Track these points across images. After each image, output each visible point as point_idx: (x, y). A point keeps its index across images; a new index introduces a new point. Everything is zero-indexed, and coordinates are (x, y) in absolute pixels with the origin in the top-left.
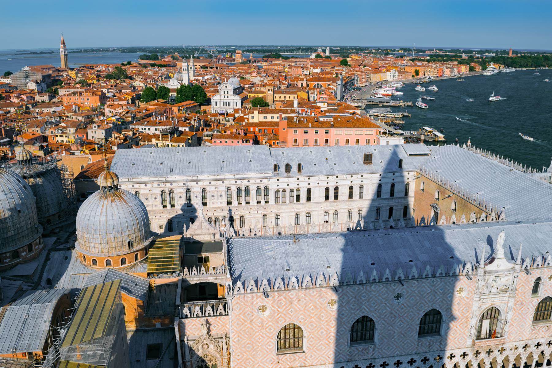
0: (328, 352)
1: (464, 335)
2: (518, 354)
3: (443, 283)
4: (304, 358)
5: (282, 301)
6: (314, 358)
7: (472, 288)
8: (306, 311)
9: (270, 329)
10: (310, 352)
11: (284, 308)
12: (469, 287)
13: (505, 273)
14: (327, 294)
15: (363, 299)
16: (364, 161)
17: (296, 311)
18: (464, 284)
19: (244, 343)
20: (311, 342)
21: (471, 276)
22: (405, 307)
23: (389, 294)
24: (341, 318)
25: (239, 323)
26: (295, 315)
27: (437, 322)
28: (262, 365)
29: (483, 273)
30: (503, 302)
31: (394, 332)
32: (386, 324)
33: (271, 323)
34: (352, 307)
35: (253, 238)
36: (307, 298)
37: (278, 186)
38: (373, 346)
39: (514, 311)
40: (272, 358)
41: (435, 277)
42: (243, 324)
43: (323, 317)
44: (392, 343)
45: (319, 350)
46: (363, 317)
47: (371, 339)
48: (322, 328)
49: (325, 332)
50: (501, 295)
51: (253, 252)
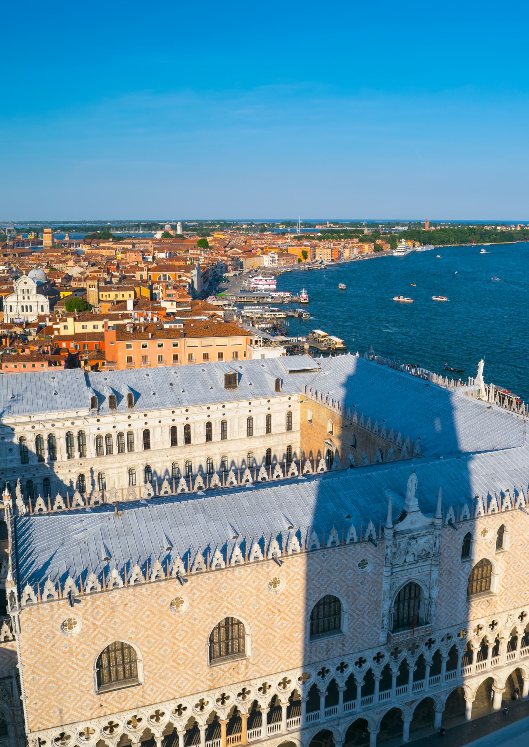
0: (175, 681)
1: (375, 628)
2: (452, 645)
3: (337, 555)
4: (141, 693)
6: (157, 691)
7: (379, 559)
8: (138, 620)
9: (84, 655)
10: (149, 682)
11: (102, 620)
12: (375, 557)
13: (423, 532)
14: (168, 591)
15: (224, 592)
16: (226, 384)
17: (123, 622)
18: (368, 554)
19: (44, 682)
20: (150, 667)
21: (376, 542)
22: (287, 597)
23: (261, 580)
24: (193, 624)
25: (33, 651)
26: (121, 628)
27: (335, 614)
28: (75, 713)
29: (392, 535)
30: (424, 573)
31: (275, 637)
32: (261, 626)
33: (84, 646)
35: (56, 514)
36: (137, 601)
37: (98, 429)
38: (244, 662)
39: (440, 585)
40: (91, 700)
41: (325, 548)
42: (40, 651)
43: (164, 626)
44: (273, 653)
45: (163, 678)
46: (227, 619)
47: (241, 652)
48: (165, 644)
49: (170, 650)
50: (421, 564)
51: (54, 535)
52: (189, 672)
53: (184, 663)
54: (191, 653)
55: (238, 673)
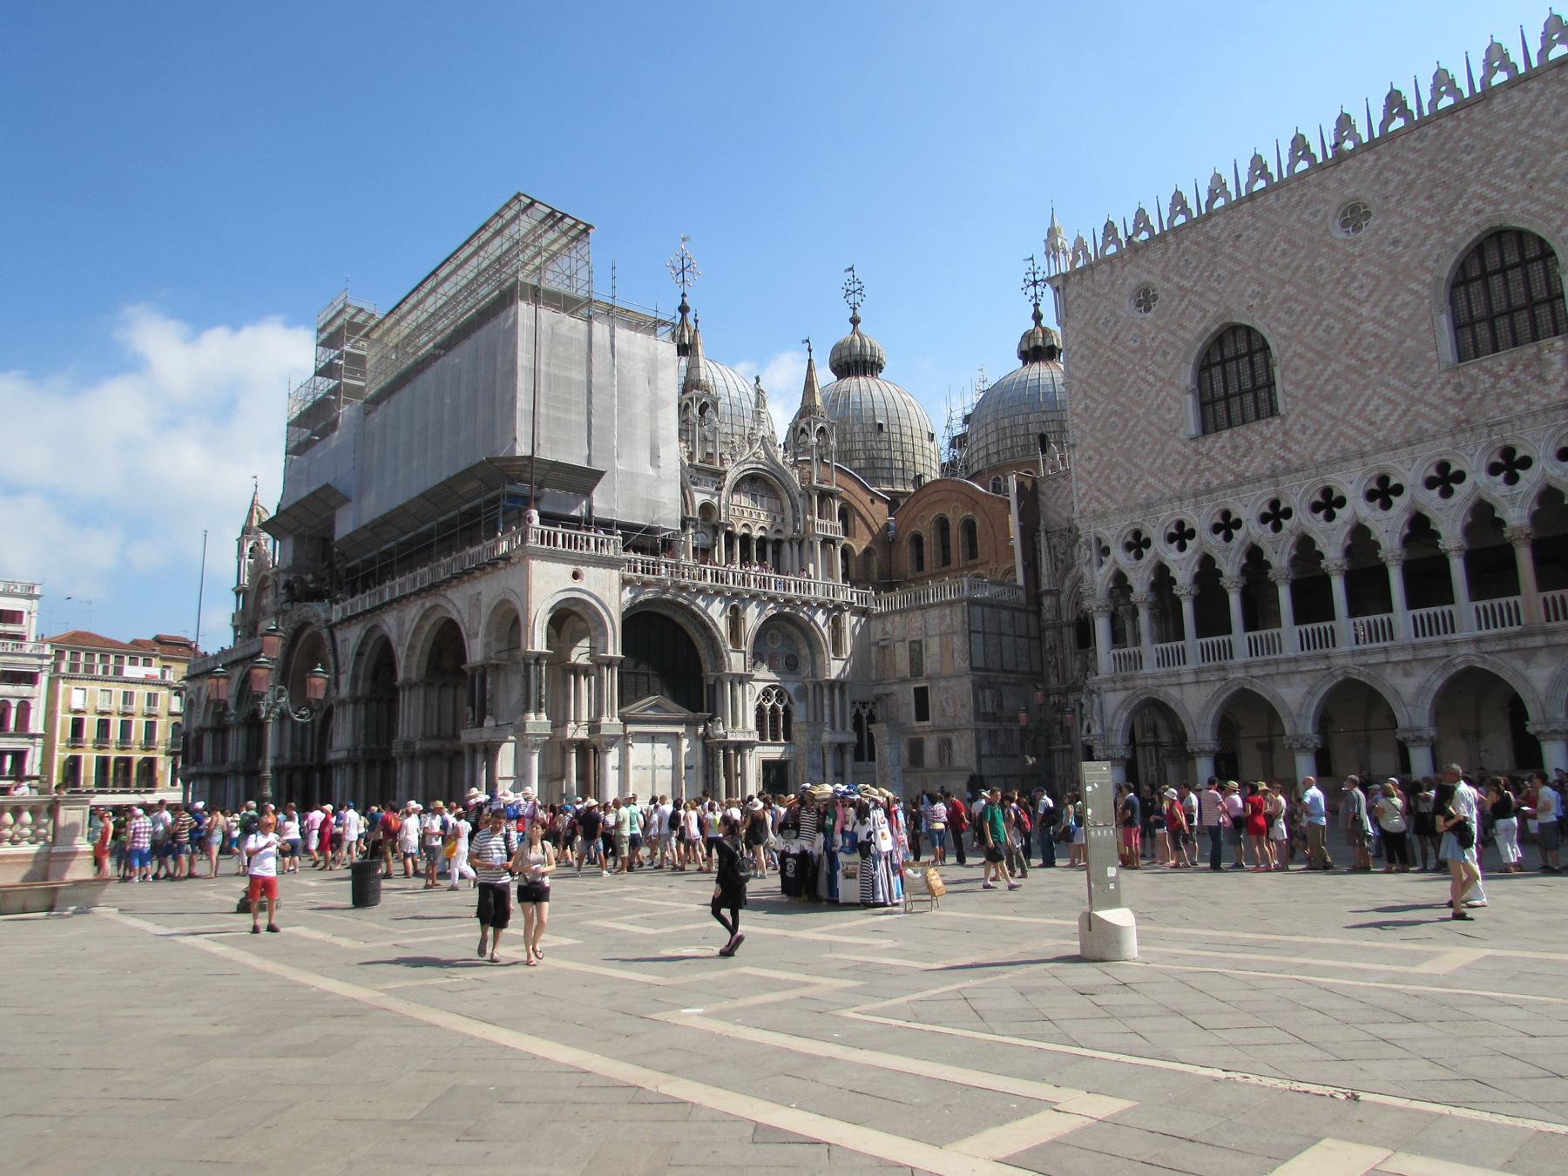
4: (1280, 437)
5: (1188, 256)
6: (1316, 432)
8: (1264, 266)
9: (1165, 354)
15: (1466, 158)
17: (1233, 274)
19: (1101, 416)
24: (1391, 257)
26: (1229, 289)
28: (1152, 480)
34: (1422, 203)
40: (1179, 453)
43: (1321, 270)
45: (1328, 399)
48: (1326, 314)
52: (1393, 381)
53: (1378, 358)
54: (1392, 330)
55: (1540, 378)
